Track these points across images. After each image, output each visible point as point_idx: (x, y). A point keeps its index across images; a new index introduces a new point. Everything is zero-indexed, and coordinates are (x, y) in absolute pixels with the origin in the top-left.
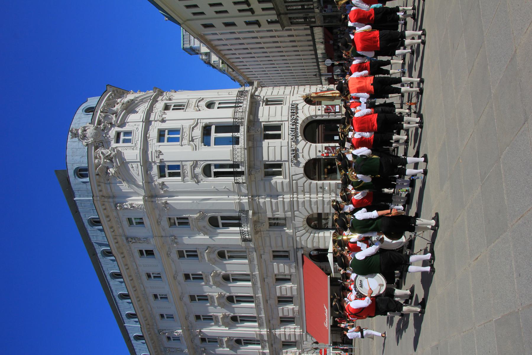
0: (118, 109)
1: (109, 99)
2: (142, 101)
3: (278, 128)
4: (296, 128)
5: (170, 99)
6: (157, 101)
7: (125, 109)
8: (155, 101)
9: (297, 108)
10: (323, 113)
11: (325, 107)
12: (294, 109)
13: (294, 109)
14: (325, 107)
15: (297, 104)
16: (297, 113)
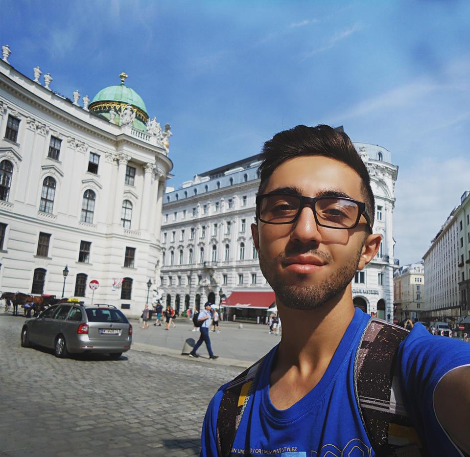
0: (379, 176)
1: (387, 168)
2: (386, 191)
3: (362, 281)
4: (361, 293)
5: (386, 210)
6: (385, 200)
7: (379, 180)
8: (385, 199)
9: (375, 294)
10: (371, 311)
11: (375, 313)
12: (376, 293)
13: (376, 293)
14: (375, 313)
15: (378, 294)
16: (372, 293)
